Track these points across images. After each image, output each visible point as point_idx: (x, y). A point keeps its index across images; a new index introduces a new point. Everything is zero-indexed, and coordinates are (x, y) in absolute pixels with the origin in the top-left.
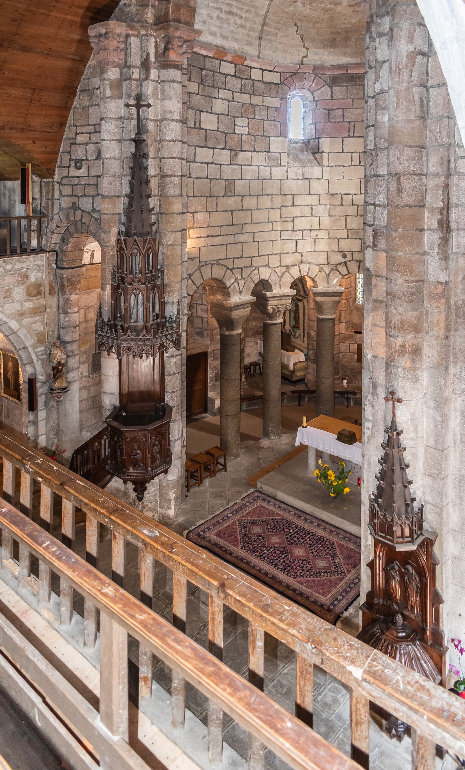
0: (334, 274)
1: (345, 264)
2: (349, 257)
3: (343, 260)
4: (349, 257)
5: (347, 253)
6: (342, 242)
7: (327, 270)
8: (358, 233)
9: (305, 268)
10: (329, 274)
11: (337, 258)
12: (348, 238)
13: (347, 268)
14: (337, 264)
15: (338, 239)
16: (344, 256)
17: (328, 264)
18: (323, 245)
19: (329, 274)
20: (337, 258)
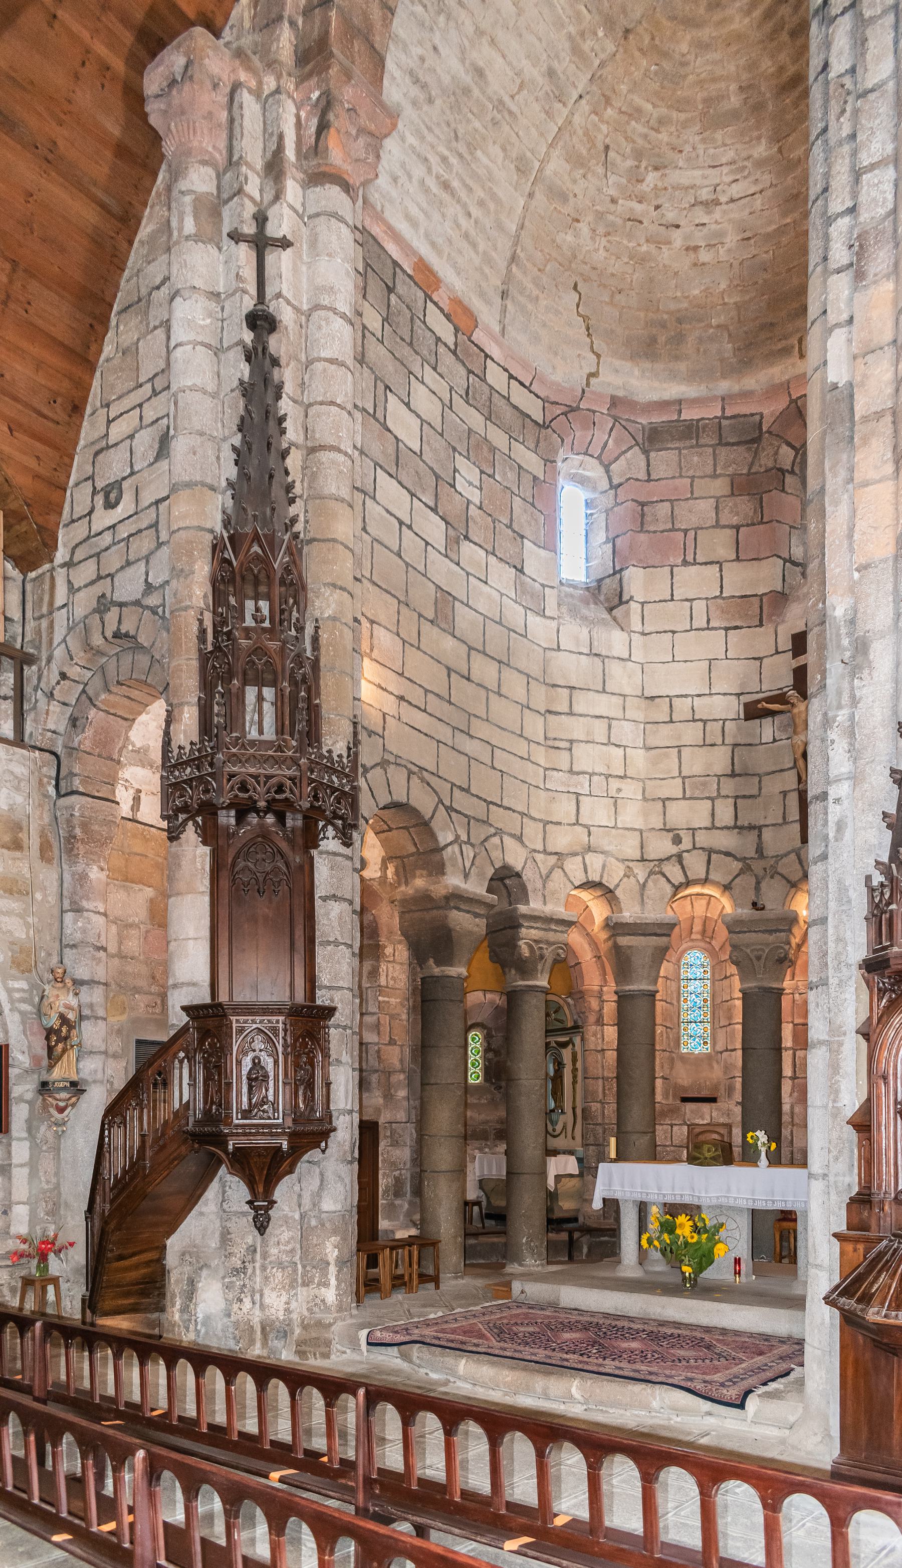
0: (655, 882)
1: (679, 857)
2: (686, 844)
3: (674, 850)
4: (686, 844)
5: (681, 833)
6: (672, 807)
7: (641, 873)
8: (704, 784)
9: (595, 861)
10: (644, 885)
11: (662, 846)
12: (684, 798)
13: (683, 868)
14: (661, 860)
15: (664, 801)
16: (677, 840)
17: (643, 860)
18: (632, 815)
19: (644, 885)
20: (662, 846)
